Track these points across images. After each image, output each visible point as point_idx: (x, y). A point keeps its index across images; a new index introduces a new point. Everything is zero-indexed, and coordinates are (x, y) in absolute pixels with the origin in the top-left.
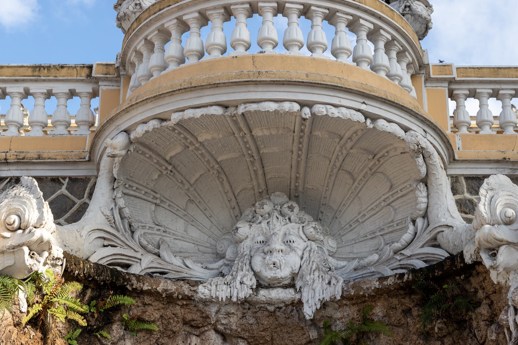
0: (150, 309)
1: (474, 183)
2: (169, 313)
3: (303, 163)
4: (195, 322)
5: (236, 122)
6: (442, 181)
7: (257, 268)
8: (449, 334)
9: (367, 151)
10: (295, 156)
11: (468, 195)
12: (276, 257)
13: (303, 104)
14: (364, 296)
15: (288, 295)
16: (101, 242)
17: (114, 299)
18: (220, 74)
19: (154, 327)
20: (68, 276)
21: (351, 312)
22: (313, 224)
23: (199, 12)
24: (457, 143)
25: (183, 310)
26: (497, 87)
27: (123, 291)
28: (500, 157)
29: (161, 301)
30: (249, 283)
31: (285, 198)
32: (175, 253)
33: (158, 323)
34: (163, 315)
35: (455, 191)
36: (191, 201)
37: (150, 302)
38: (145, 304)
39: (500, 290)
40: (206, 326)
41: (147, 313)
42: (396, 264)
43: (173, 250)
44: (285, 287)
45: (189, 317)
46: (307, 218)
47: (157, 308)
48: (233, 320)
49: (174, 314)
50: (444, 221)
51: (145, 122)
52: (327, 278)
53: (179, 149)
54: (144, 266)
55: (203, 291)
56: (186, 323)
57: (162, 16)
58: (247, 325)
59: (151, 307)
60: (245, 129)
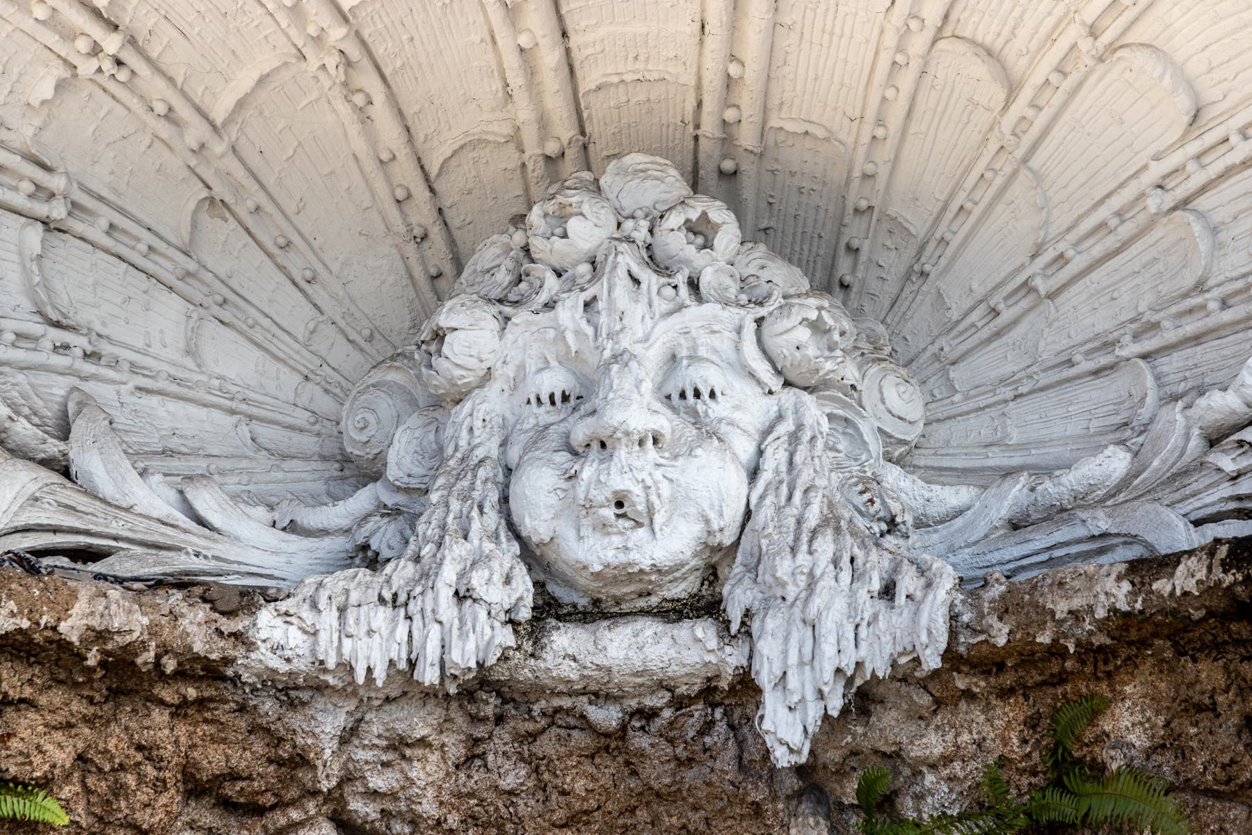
2: (116, 742)
4: (240, 785)
7: (537, 526)
12: (629, 472)
14: (1056, 651)
15: (687, 650)
21: (994, 729)
22: (811, 307)
25: (182, 730)
29: (76, 685)
30: (498, 596)
31: (673, 184)
32: (145, 459)
33: (66, 792)
34: (91, 754)
37: (28, 692)
40: (292, 803)
41: (14, 744)
42: (1216, 496)
44: (673, 612)
45: (213, 760)
47: (60, 718)
49: (140, 748)
52: (877, 567)
56: (197, 787)
58: (490, 796)
59: (32, 715)
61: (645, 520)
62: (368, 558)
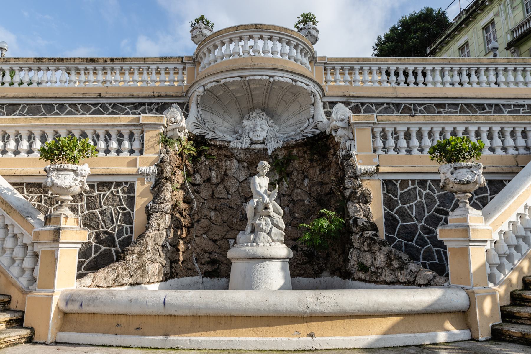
0: (214, 151)
1: (332, 105)
2: (220, 153)
3: (267, 98)
5: (244, 83)
7: (251, 137)
8: (320, 160)
9: (292, 93)
10: (265, 95)
11: (329, 109)
12: (258, 133)
13: (270, 76)
15: (262, 146)
16: (195, 127)
17: (202, 147)
18: (239, 65)
19: (215, 157)
20: (189, 139)
21: (285, 152)
22: (271, 121)
23: (230, 39)
24: (326, 89)
27: (205, 145)
30: (248, 142)
31: (260, 111)
32: (220, 131)
35: (324, 108)
36: (225, 112)
38: (212, 149)
43: (221, 129)
44: (261, 144)
45: (227, 154)
46: (269, 118)
48: (242, 155)
51: (211, 83)
53: (222, 92)
54: (210, 136)
55: (232, 145)
56: (225, 156)
57: (215, 40)
60: (247, 85)
62: (237, 139)
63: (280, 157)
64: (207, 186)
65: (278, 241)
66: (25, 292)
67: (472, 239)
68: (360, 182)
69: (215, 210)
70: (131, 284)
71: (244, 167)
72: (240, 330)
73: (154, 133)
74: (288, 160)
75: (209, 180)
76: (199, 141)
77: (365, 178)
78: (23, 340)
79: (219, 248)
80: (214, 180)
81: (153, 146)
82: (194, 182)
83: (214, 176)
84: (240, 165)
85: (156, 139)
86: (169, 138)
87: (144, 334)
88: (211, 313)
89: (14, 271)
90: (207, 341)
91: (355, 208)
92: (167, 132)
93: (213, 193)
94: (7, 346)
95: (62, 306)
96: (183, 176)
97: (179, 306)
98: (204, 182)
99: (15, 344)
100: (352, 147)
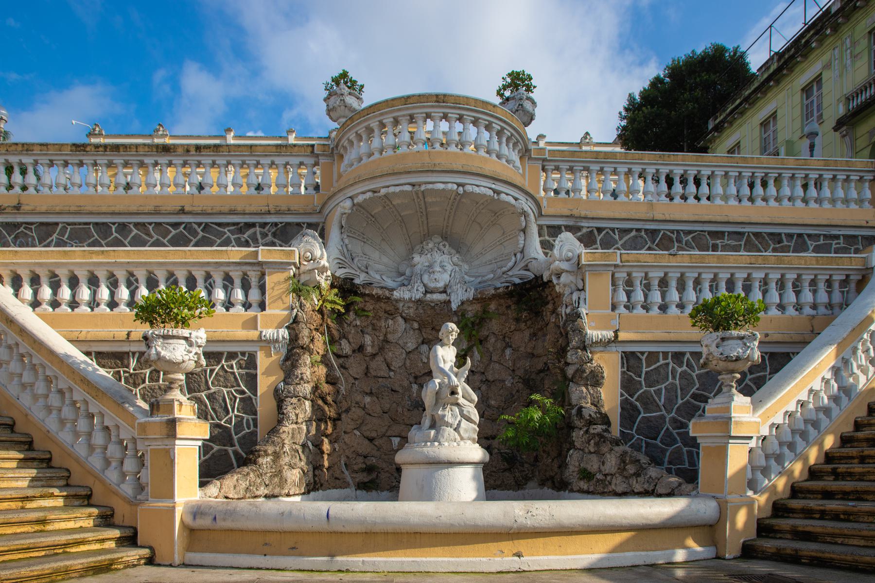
2: (377, 306)
6: (534, 229)
7: (425, 282)
8: (530, 319)
12: (437, 276)
15: (443, 297)
19: (370, 314)
20: (332, 286)
22: (457, 256)
26: (572, 164)
27: (356, 294)
28: (568, 213)
39: (560, 296)
43: (377, 270)
44: (441, 292)
45: (388, 309)
46: (453, 251)
48: (412, 311)
50: (533, 255)
52: (465, 287)
54: (361, 279)
55: (396, 294)
56: (385, 312)
61: (438, 282)
62: (404, 285)
63: (470, 315)
64: (358, 359)
65: (469, 439)
66: (134, 503)
67: (732, 434)
68: (590, 355)
69: (371, 394)
70: (266, 496)
71: (414, 330)
72: (427, 549)
73: (280, 277)
74: (482, 319)
75: (361, 349)
76: (346, 288)
77: (597, 349)
78: (143, 561)
79: (378, 450)
80: (369, 349)
81: (280, 298)
82: (340, 353)
83: (369, 343)
84: (408, 326)
85: (284, 286)
86: (303, 284)
87: (301, 555)
88: (390, 529)
89: (112, 475)
90: (386, 562)
91: (580, 394)
92: (299, 275)
93: (367, 368)
94: (125, 568)
95: (189, 520)
96: (325, 343)
97: (347, 521)
98: (354, 351)
99: (134, 566)
100: (582, 302)
